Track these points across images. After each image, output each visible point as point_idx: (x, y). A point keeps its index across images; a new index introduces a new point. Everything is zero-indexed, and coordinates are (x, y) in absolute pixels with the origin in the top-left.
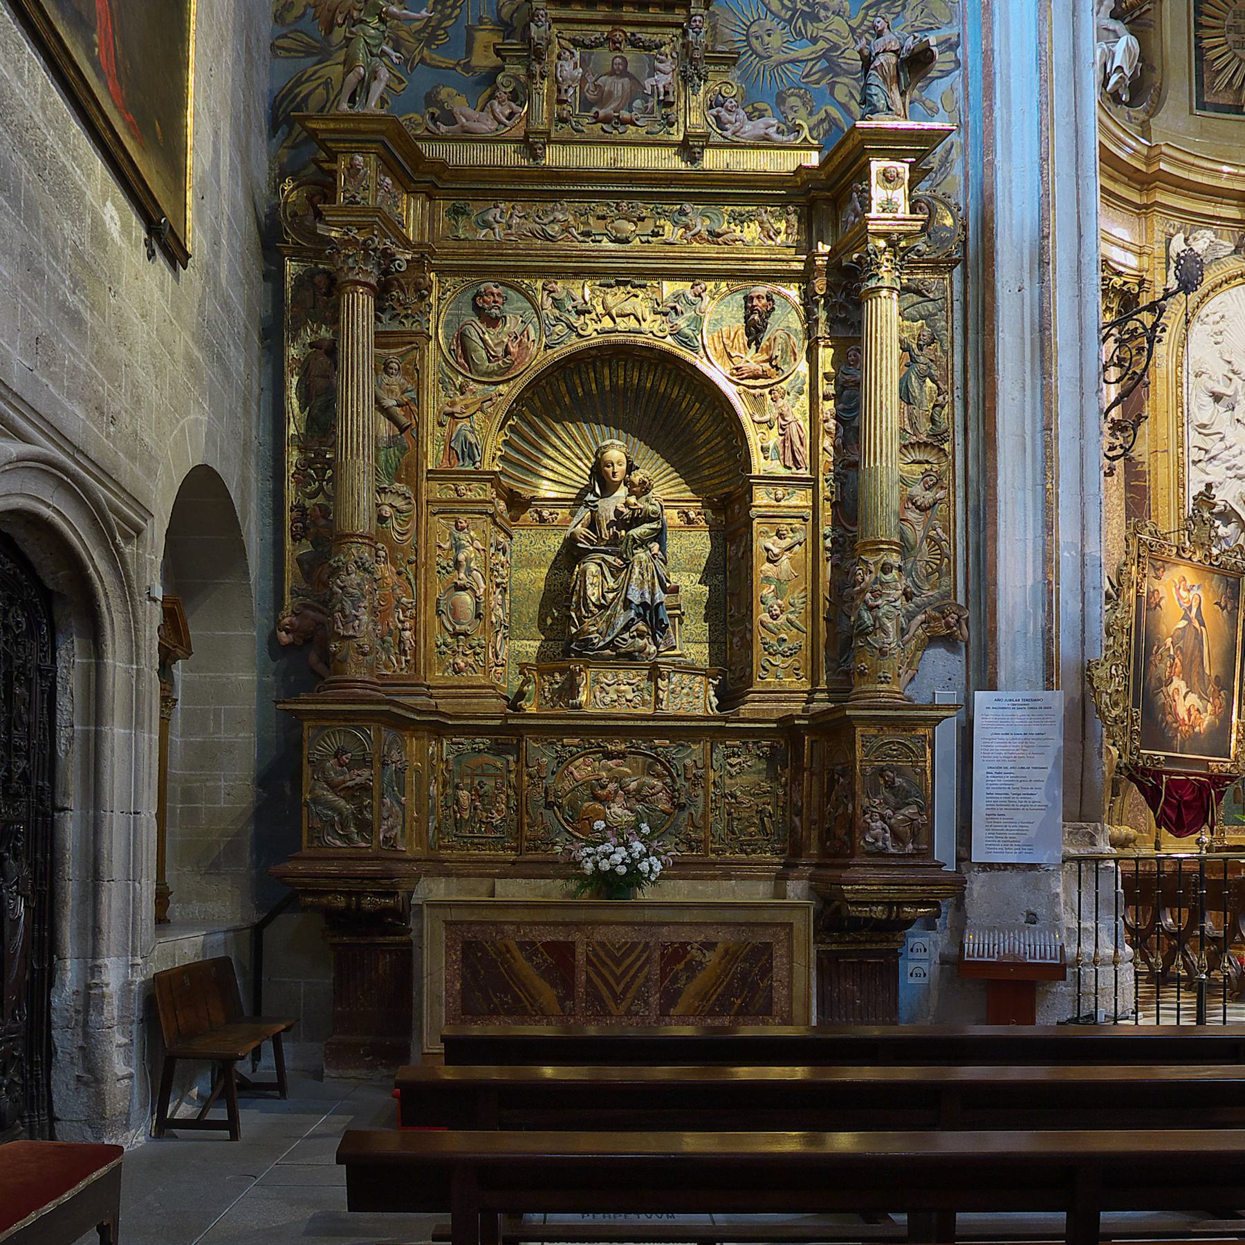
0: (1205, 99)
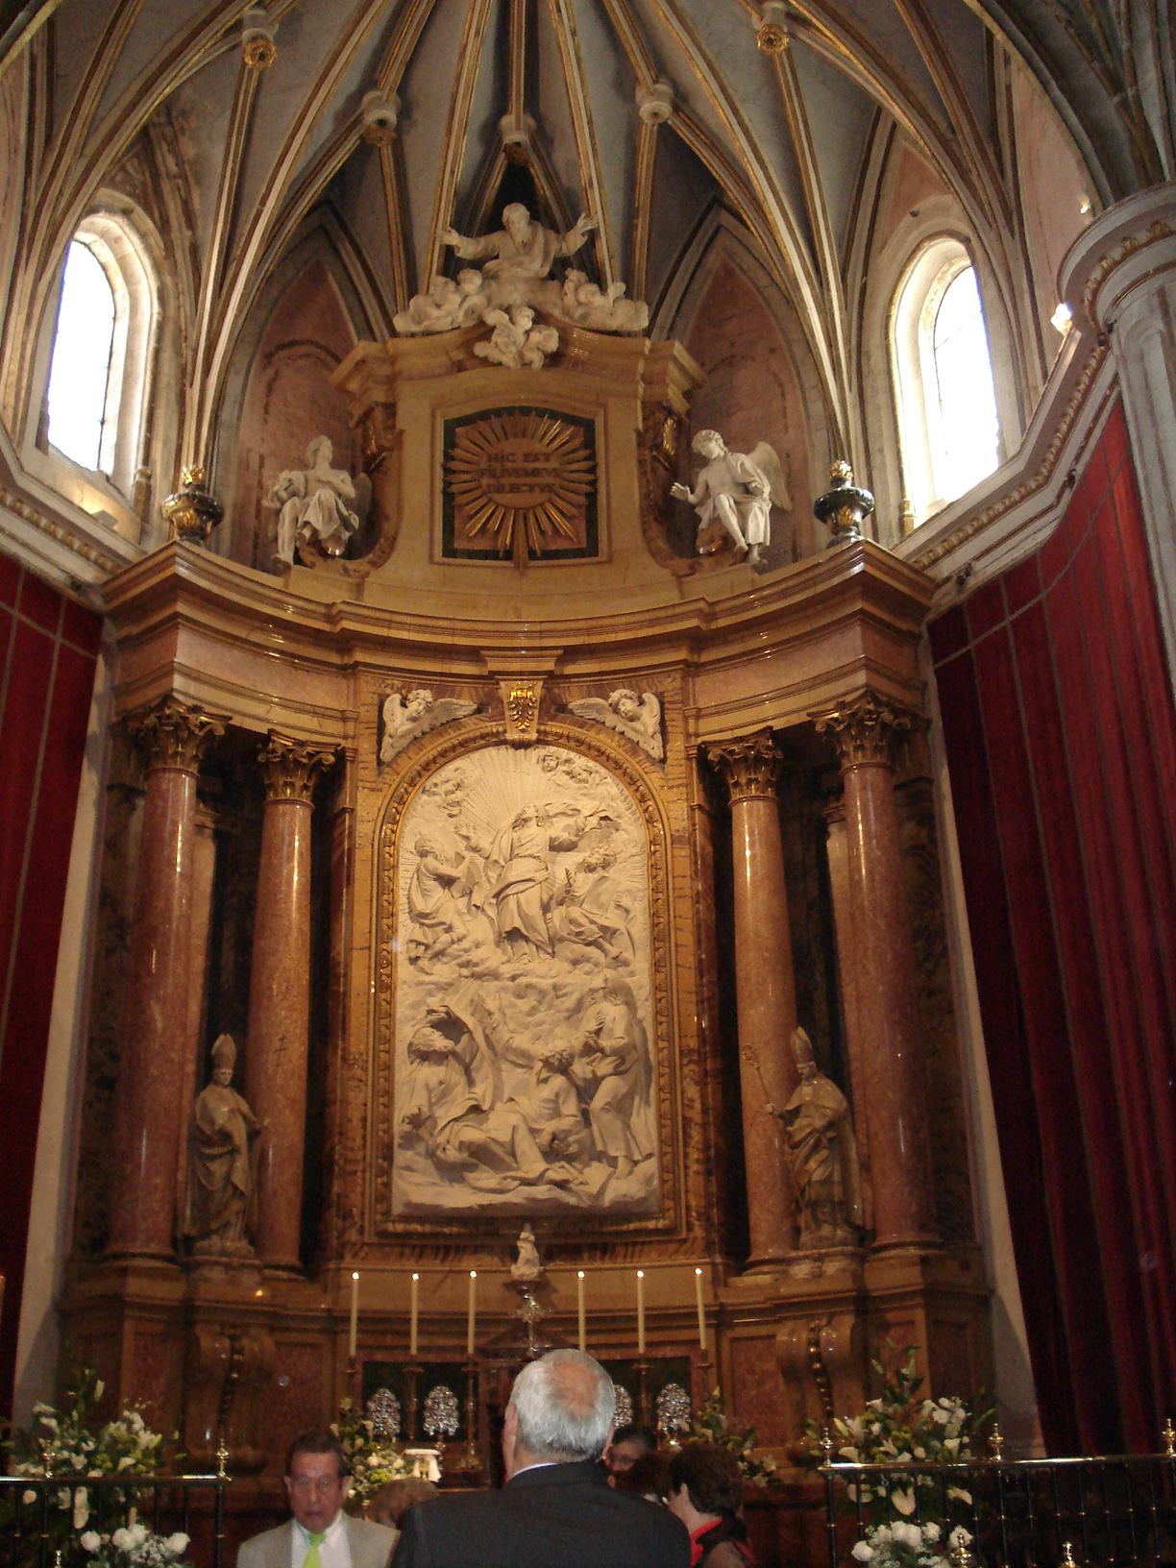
0: (456, 546)
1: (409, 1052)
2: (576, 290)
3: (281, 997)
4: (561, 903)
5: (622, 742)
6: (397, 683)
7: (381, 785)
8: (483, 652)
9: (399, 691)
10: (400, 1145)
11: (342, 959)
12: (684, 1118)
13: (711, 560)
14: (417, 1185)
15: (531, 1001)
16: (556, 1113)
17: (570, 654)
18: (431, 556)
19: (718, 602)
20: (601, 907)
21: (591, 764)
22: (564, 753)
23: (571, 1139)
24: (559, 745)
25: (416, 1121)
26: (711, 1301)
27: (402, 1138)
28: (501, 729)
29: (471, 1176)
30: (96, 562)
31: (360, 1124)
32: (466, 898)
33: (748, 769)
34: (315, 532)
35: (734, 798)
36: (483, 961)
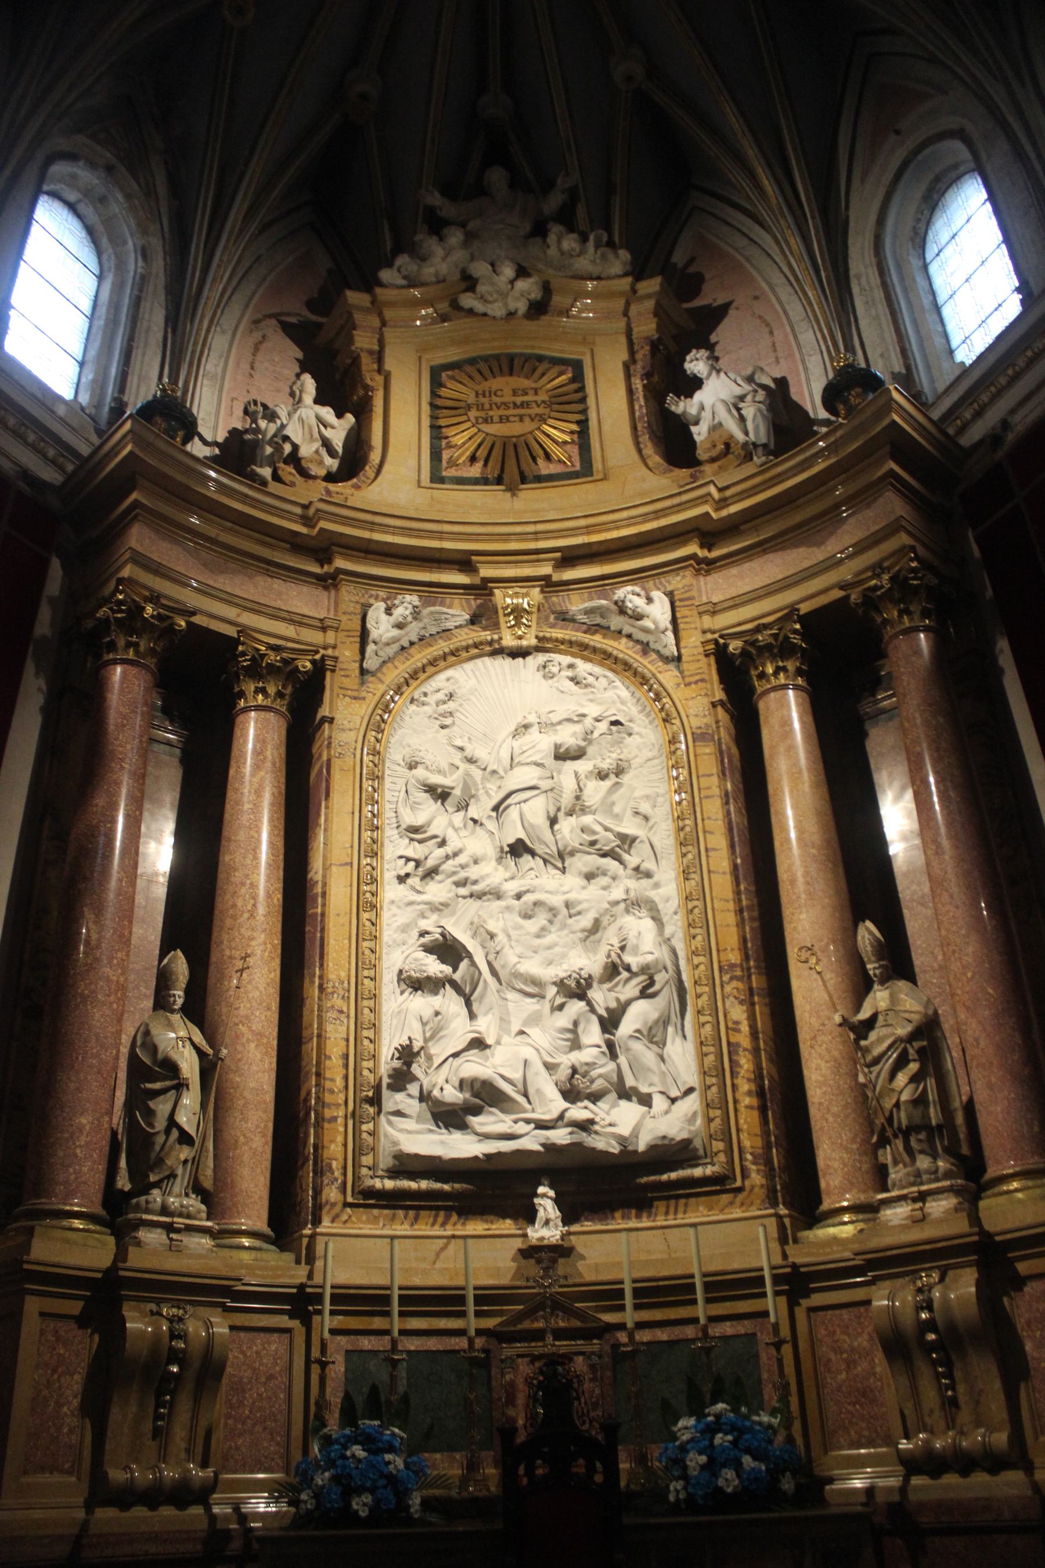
1: (399, 980)
2: (559, 241)
3: (246, 915)
4: (570, 813)
5: (631, 644)
6: (382, 594)
7: (364, 694)
8: (474, 558)
9: (384, 600)
10: (390, 1087)
11: (319, 877)
12: (729, 1043)
13: (715, 465)
14: (409, 1132)
15: (541, 919)
16: (576, 1045)
17: (570, 558)
18: (419, 481)
19: (727, 487)
20: (617, 817)
21: (597, 670)
22: (567, 660)
23: (594, 1073)
24: (560, 652)
25: (407, 1054)
26: (778, 1260)
27: (390, 1076)
28: (496, 637)
29: (474, 1121)
30: (53, 462)
31: (341, 1062)
32: (462, 813)
33: (773, 658)
34: (296, 447)
35: (759, 690)
36: (483, 878)
